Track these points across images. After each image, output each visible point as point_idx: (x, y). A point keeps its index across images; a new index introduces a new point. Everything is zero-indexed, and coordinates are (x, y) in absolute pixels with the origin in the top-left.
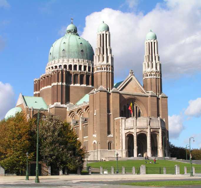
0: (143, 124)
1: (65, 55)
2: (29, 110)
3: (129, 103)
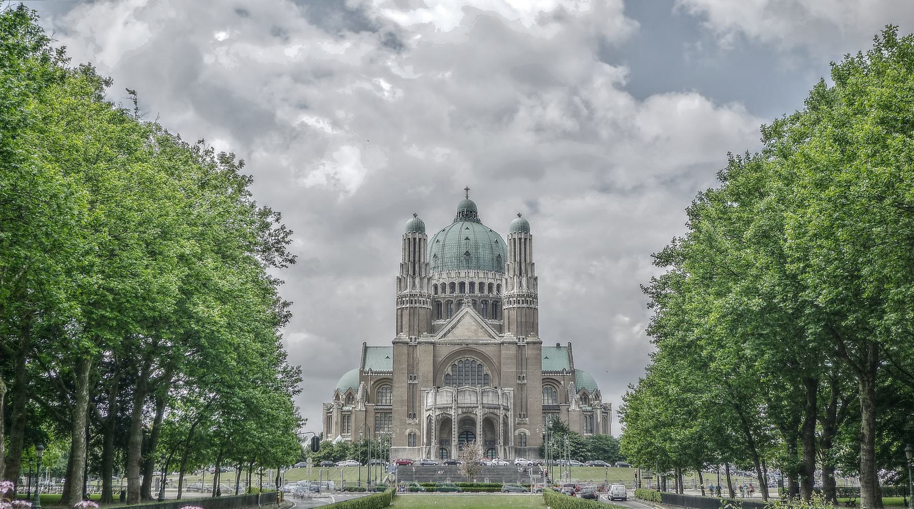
0: (447, 400)
2: (364, 375)
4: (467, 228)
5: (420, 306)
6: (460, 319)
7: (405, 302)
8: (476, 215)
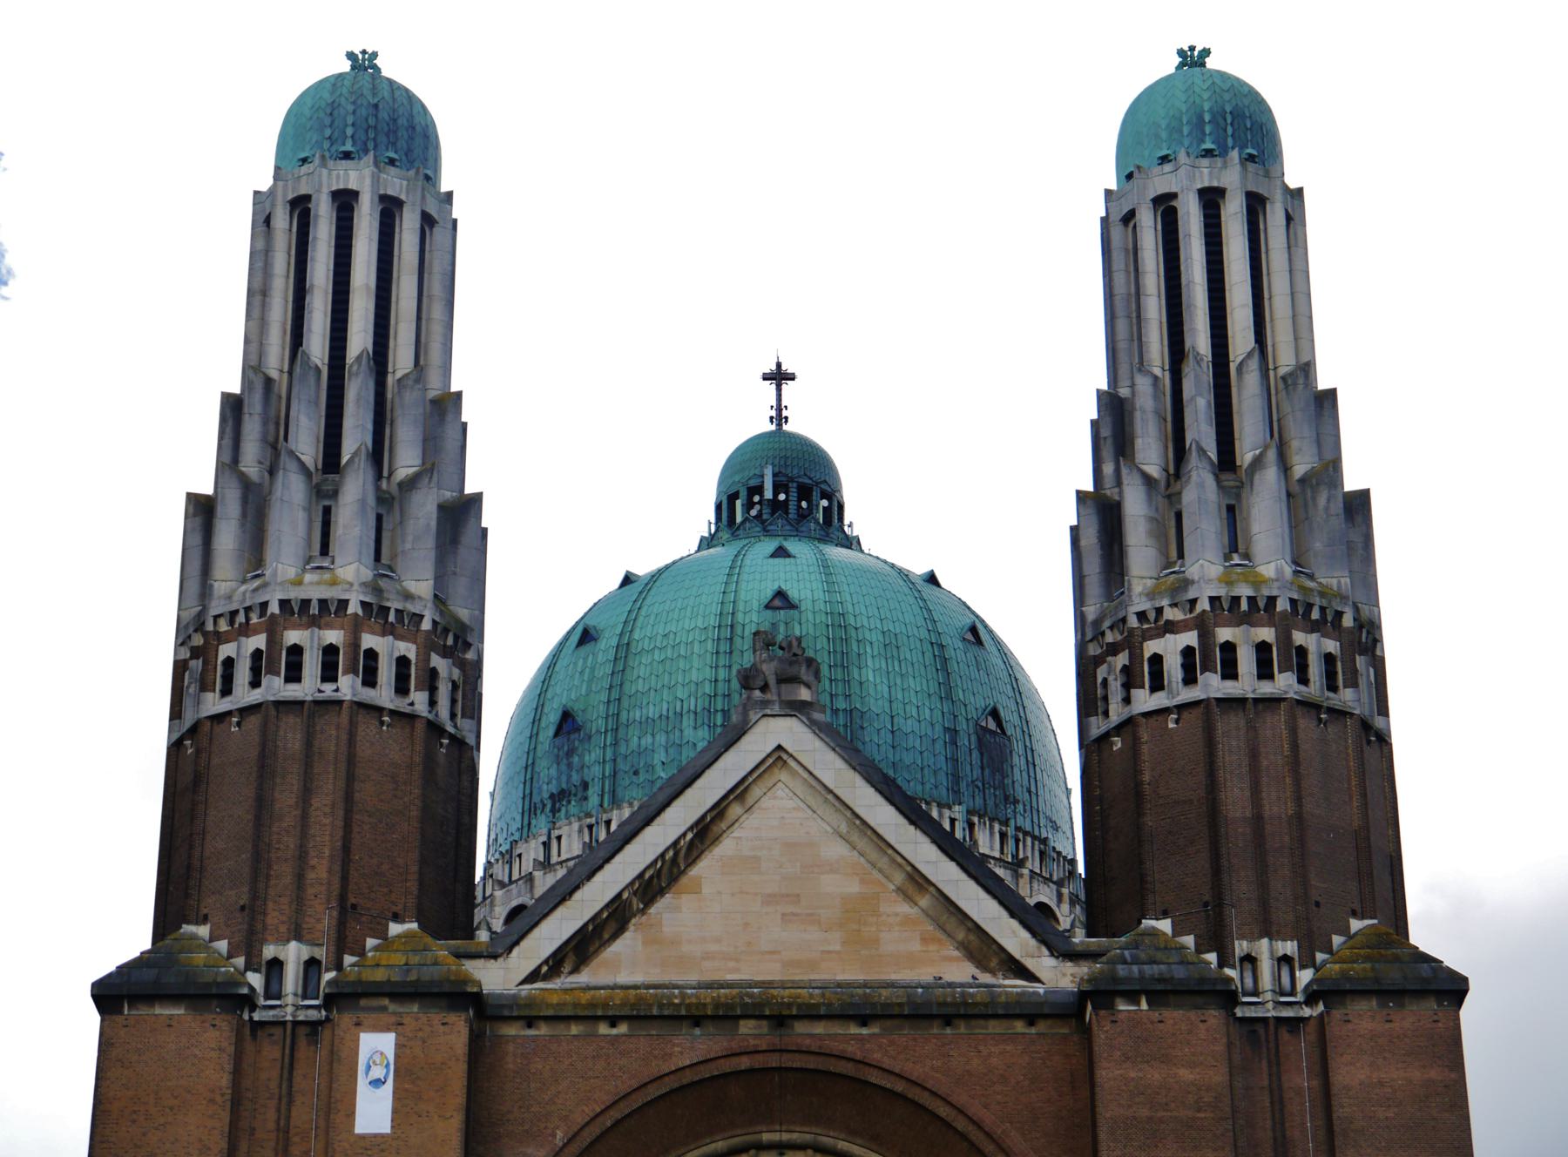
1: (576, 778)
4: (781, 552)
5: (368, 695)
6: (719, 810)
7: (242, 674)
8: (836, 510)
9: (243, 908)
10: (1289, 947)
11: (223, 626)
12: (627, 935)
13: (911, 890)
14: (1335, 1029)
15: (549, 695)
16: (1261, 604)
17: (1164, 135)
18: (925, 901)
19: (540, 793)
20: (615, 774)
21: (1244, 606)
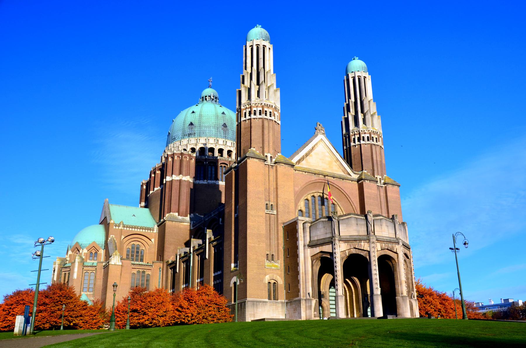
0: (358, 231)
2: (114, 227)
3: (316, 195)
4: (221, 106)
6: (315, 146)
9: (261, 147)
10: (381, 177)
11: (254, 105)
12: (304, 161)
13: (336, 161)
14: (387, 188)
15: (187, 119)
16: (376, 133)
17: (358, 68)
18: (338, 163)
19: (186, 133)
20: (200, 133)
21: (375, 132)
